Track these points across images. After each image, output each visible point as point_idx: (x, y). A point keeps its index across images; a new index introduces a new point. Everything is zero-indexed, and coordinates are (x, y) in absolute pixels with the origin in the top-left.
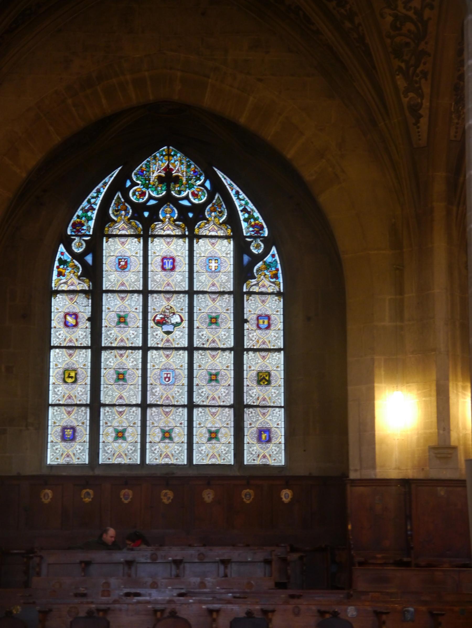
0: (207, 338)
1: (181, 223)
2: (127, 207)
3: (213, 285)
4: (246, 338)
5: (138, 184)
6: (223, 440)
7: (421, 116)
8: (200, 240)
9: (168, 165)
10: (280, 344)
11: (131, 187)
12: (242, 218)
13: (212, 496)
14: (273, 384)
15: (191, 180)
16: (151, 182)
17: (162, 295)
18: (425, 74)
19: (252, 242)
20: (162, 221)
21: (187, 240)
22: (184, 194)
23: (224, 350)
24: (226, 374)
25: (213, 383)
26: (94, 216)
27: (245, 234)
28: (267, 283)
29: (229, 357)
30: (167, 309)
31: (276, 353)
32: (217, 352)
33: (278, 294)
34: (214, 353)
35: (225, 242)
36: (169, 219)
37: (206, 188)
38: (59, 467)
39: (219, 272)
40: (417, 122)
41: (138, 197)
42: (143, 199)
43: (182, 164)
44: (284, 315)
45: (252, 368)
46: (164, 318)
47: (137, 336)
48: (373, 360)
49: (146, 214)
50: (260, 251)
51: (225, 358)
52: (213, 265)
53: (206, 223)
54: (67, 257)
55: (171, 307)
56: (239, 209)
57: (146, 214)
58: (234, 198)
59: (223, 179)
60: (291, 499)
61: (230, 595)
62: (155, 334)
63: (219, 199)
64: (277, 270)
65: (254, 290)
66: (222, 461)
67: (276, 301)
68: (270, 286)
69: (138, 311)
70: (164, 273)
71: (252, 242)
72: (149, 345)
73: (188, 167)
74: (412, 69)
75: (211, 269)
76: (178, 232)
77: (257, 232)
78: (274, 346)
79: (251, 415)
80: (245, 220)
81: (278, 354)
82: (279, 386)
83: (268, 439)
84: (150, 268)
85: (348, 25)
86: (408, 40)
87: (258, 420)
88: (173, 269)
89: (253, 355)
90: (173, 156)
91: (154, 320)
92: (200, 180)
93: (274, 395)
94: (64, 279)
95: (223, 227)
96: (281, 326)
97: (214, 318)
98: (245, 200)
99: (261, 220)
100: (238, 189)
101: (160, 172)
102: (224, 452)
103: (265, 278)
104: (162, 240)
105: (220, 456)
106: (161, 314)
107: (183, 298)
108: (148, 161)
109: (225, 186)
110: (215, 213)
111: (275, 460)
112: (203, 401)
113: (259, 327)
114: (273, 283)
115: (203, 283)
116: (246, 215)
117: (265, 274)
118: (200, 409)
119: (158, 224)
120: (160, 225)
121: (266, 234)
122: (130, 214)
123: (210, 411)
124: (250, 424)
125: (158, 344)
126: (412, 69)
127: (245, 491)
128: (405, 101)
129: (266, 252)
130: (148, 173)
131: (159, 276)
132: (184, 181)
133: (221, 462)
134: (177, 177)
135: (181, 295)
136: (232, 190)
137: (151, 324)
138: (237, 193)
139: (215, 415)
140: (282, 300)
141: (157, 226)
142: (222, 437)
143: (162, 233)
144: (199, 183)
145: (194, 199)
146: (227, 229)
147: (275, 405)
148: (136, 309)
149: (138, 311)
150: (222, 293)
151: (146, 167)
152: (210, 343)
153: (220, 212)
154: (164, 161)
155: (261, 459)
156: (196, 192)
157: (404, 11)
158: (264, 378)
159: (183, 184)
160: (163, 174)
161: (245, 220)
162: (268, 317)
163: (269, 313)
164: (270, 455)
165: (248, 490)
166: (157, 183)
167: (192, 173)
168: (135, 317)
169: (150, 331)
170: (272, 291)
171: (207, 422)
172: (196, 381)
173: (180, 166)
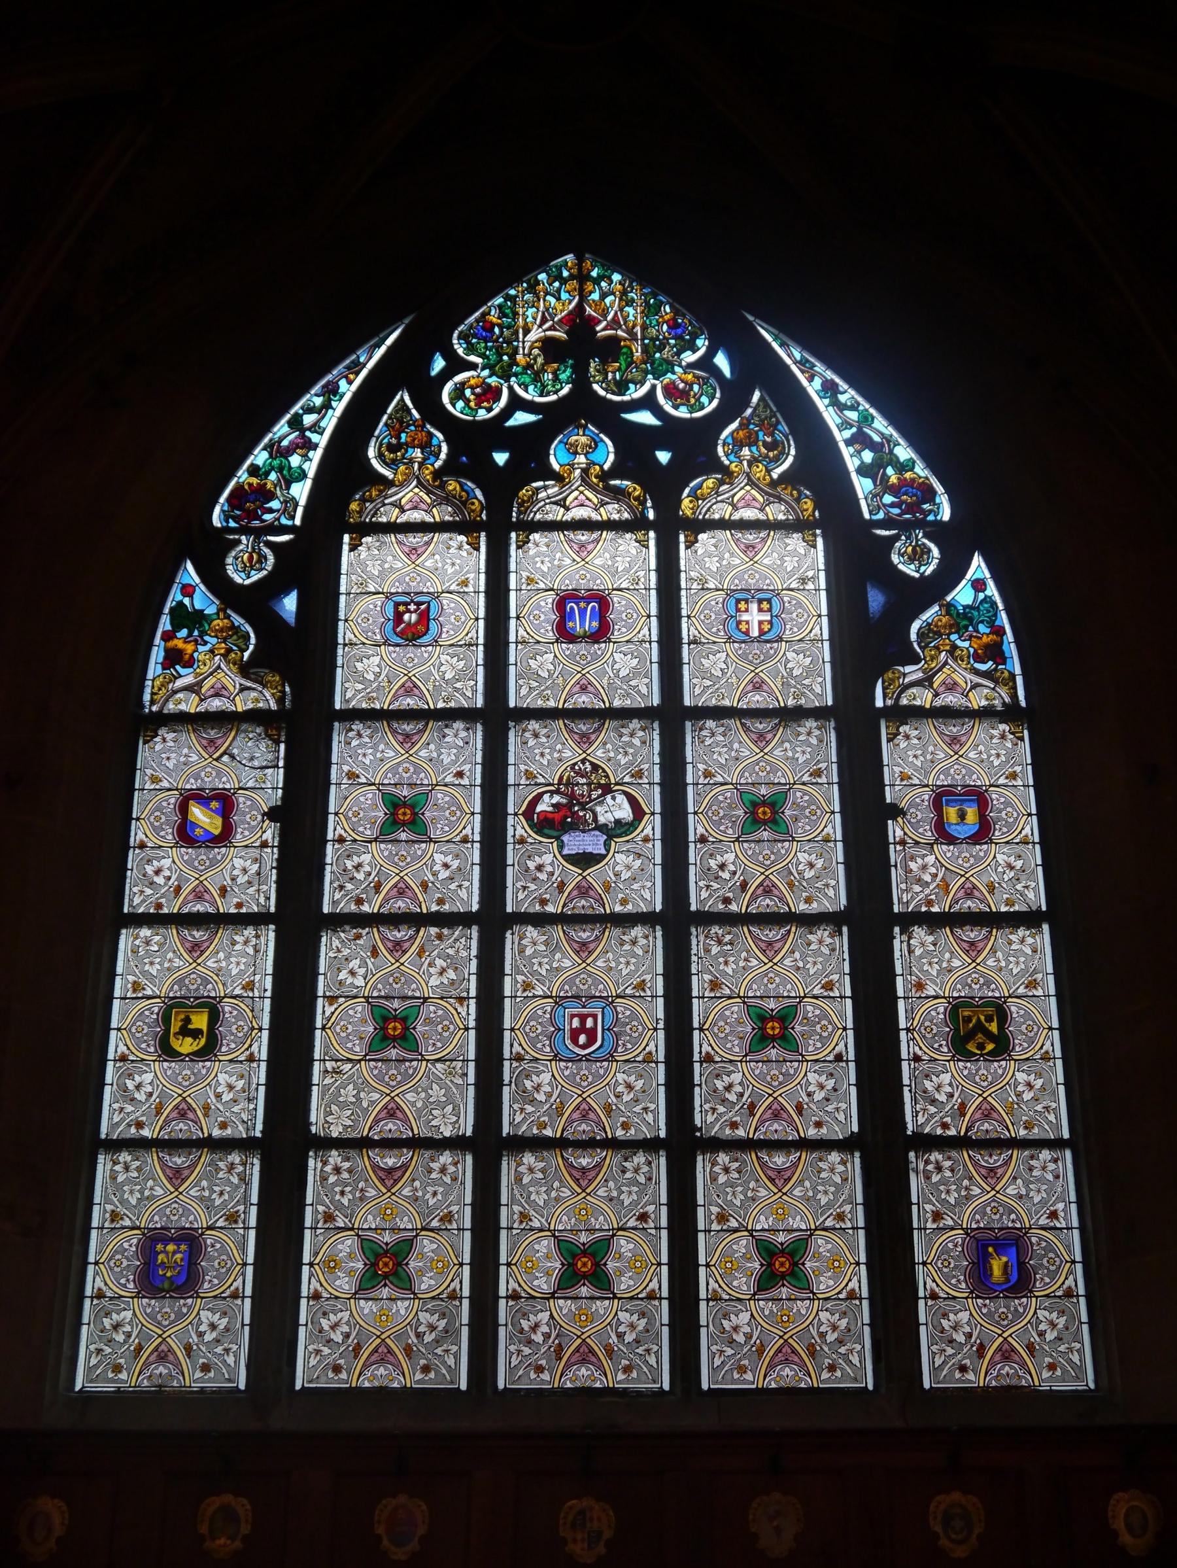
2: (431, 435)
3: (758, 686)
6: (824, 1284)
8: (702, 537)
9: (580, 308)
10: (1035, 895)
11: (446, 375)
12: (852, 464)
16: (519, 357)
19: (896, 538)
20: (559, 478)
22: (636, 393)
23: (810, 921)
24: (824, 1015)
26: (311, 468)
28: (963, 677)
30: (580, 774)
32: (783, 931)
33: (1010, 714)
35: (795, 542)
37: (716, 372)
39: (780, 640)
41: (472, 404)
42: (489, 410)
43: (630, 303)
46: (570, 805)
50: (929, 570)
51: (817, 953)
52: (754, 617)
53: (722, 482)
54: (203, 601)
55: (595, 767)
56: (841, 436)
58: (821, 404)
62: (531, 865)
63: (767, 406)
65: (918, 703)
67: (1003, 737)
68: (975, 686)
69: (465, 781)
73: (650, 310)
75: (747, 633)
76: (613, 511)
77: (912, 508)
78: (1009, 903)
79: (935, 1178)
80: (863, 471)
81: (1028, 933)
82: (1046, 1057)
83: (1014, 1278)
87: (968, 1198)
89: (930, 939)
90: (597, 281)
91: (529, 813)
92: (694, 350)
93: (1027, 1096)
94: (187, 677)
96: (1031, 828)
97: (764, 804)
98: (861, 408)
100: (830, 375)
101: (549, 329)
102: (831, 1337)
103: (955, 659)
105: (812, 1352)
106: (557, 792)
107: (641, 733)
108: (508, 298)
109: (787, 367)
110: (754, 449)
111: (1052, 1367)
112: (734, 1125)
115: (715, 680)
116: (868, 456)
117: (954, 647)
119: (545, 488)
121: (946, 514)
123: (763, 1165)
124: (937, 1216)
129: (951, 573)
132: (638, 355)
133: (824, 1379)
136: (811, 379)
137: (516, 827)
139: (789, 1179)
141: (542, 495)
143: (558, 514)
144: (689, 357)
145: (676, 407)
146: (798, 500)
148: (460, 774)
149: (465, 781)
151: (503, 315)
152: (754, 898)
153: (770, 447)
154: (564, 296)
155: (992, 1364)
158: (980, 1027)
159: (632, 362)
162: (980, 797)
163: (980, 779)
164: (1030, 1348)
166: (540, 360)
168: (454, 801)
170: (984, 703)
173: (621, 310)
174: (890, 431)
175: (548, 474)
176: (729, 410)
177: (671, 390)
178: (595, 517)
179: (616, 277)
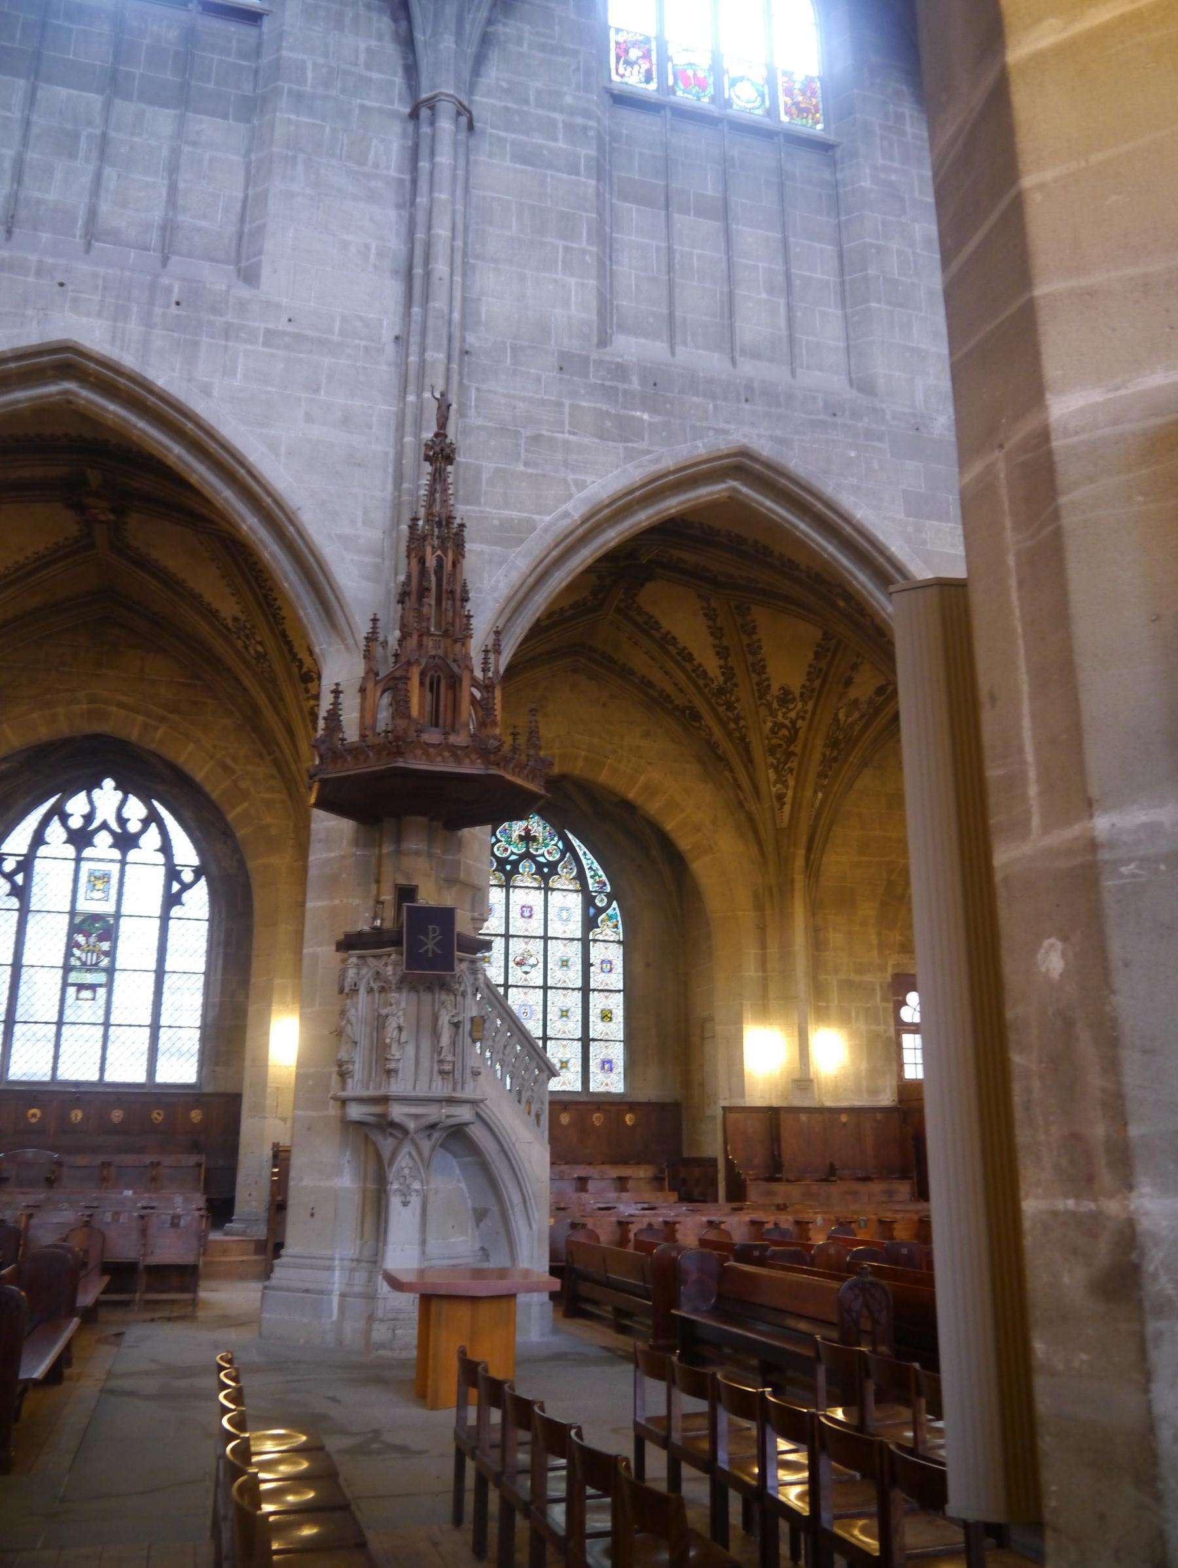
3: (565, 932)
4: (591, 980)
7: (785, 804)
14: (614, 1020)
17: (521, 939)
18: (791, 770)
21: (543, 892)
22: (540, 852)
23: (573, 989)
25: (564, 1019)
28: (610, 933)
33: (619, 942)
34: (565, 992)
35: (575, 894)
40: (781, 808)
44: (624, 960)
47: (618, 981)
48: (741, 1005)
52: (564, 915)
56: (586, 867)
57: (508, 867)
58: (582, 858)
73: (545, 828)
74: (781, 766)
76: (535, 884)
77: (601, 888)
80: (592, 877)
85: (732, 725)
86: (781, 742)
88: (530, 917)
96: (621, 970)
99: (604, 878)
104: (522, 891)
113: (602, 971)
116: (592, 873)
118: (553, 1041)
120: (519, 877)
126: (781, 766)
127: (596, 1115)
128: (774, 790)
129: (609, 905)
132: (541, 841)
134: (535, 836)
137: (511, 964)
144: (553, 842)
150: (573, 939)
160: (523, 834)
161: (592, 877)
162: (610, 962)
169: (510, 970)
174: (599, 867)
175: (519, 873)
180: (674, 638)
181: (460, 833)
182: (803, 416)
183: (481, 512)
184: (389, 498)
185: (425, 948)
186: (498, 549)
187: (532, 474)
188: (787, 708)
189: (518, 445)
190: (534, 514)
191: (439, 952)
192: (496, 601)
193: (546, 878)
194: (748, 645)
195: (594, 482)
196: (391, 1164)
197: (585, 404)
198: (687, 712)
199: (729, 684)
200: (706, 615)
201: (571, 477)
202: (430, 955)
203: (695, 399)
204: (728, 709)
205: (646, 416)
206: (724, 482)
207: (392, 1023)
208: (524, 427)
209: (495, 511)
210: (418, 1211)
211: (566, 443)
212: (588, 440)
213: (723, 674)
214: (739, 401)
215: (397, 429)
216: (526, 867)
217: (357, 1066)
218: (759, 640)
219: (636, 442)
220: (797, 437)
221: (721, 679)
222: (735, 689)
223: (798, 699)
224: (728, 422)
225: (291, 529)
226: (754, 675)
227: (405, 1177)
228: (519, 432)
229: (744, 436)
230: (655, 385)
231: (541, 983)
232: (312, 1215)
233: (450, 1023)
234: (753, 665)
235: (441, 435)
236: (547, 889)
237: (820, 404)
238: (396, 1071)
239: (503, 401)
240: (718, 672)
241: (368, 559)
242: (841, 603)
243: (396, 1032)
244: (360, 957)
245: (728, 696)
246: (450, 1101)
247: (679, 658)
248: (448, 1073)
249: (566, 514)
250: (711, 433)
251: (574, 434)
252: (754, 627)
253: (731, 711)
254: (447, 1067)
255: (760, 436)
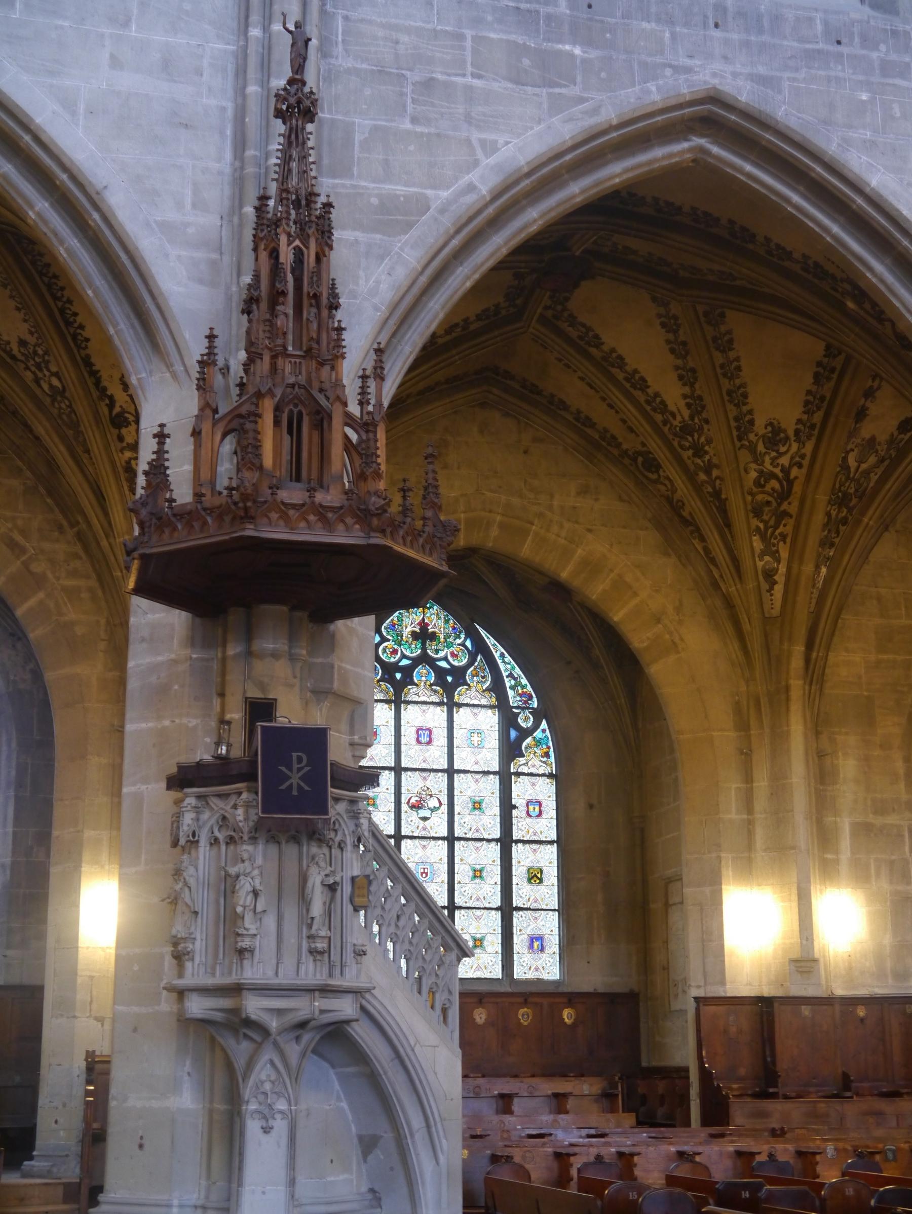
0: (469, 826)
1: (438, 688)
3: (476, 763)
4: (514, 827)
5: (389, 640)
7: (775, 583)
9: (423, 619)
12: (508, 685)
13: (484, 1017)
14: (546, 882)
15: (449, 637)
17: (417, 773)
19: (520, 713)
20: (417, 685)
22: (441, 654)
23: (489, 841)
24: (492, 870)
25: (477, 881)
27: (511, 705)
28: (538, 763)
29: (495, 850)
31: (549, 846)
33: (550, 776)
34: (478, 844)
36: (425, 683)
38: (527, 982)
39: (483, 747)
40: (772, 588)
43: (440, 618)
44: (557, 801)
45: (522, 864)
48: (719, 858)
49: (398, 676)
50: (529, 725)
51: (491, 851)
52: (476, 739)
53: (467, 690)
55: (428, 788)
56: (505, 674)
58: (499, 661)
59: (485, 638)
60: (575, 1019)
61: (645, 1135)
62: (409, 820)
64: (549, 748)
66: (489, 974)
68: (541, 766)
69: (389, 791)
70: (420, 747)
71: (520, 713)
72: (403, 834)
73: (447, 622)
74: (770, 531)
76: (435, 699)
77: (526, 702)
78: (546, 837)
79: (521, 919)
80: (512, 688)
83: (540, 948)
84: (403, 740)
85: (702, 477)
86: (770, 499)
88: (430, 742)
90: (429, 609)
91: (408, 803)
92: (460, 638)
95: (487, 694)
96: (553, 814)
100: (503, 650)
101: (414, 627)
108: (400, 613)
112: (466, 902)
114: (544, 762)
118: (463, 911)
120: (414, 689)
121: (535, 705)
122: (380, 675)
125: (413, 832)
126: (770, 531)
127: (522, 1011)
128: (760, 564)
130: (400, 628)
131: (414, 750)
132: (442, 640)
133: (488, 976)
134: (434, 633)
135: (440, 774)
136: (496, 652)
137: (404, 807)
138: (502, 655)
140: (554, 783)
141: (411, 691)
142: (488, 946)
143: (416, 699)
144: (458, 641)
147: (549, 907)
148: (387, 789)
149: (389, 791)
150: (487, 773)
151: (399, 620)
152: (473, 833)
153: (483, 677)
154: (418, 614)
156: (456, 653)
157: (771, 468)
158: (535, 875)
161: (512, 688)
163: (540, 798)
164: (543, 968)
165: (525, 1009)
166: (411, 639)
167: (451, 629)
168: (386, 798)
169: (403, 816)
170: (543, 772)
171: (471, 927)
172: (457, 878)
174: (521, 673)
176: (471, 663)
177: (453, 654)
178: (428, 700)
179: (435, 607)
180: (620, 357)
181: (332, 627)
182: (796, 44)
183: (354, 187)
184: (228, 170)
185: (287, 784)
186: (378, 236)
187: (422, 133)
188: (777, 451)
189: (402, 94)
190: (425, 188)
191: (307, 788)
192: (376, 309)
193: (449, 690)
194: (722, 366)
195: (507, 143)
196: (246, 1077)
197: (493, 35)
198: (640, 459)
199: (696, 420)
200: (663, 325)
201: (476, 136)
202: (295, 793)
203: (645, 25)
204: (695, 455)
205: (577, 51)
206: (687, 140)
207: (245, 886)
208: (410, 70)
209: (372, 185)
210: (284, 1141)
211: (469, 88)
212: (499, 86)
213: (688, 406)
214: (705, 25)
215: (237, 75)
216: (423, 674)
217: (198, 943)
218: (737, 359)
219: (565, 86)
220: (787, 75)
221: (686, 413)
222: (706, 427)
223: (793, 438)
224: (691, 57)
225: (96, 216)
226: (730, 407)
227: (265, 1094)
228: (403, 75)
229: (714, 75)
230: (590, 6)
231: (444, 833)
232: (141, 1146)
233: (323, 884)
234: (729, 393)
235: (297, 81)
236: (451, 706)
237: (820, 28)
238: (251, 951)
239: (381, 33)
240: (682, 403)
241: (199, 255)
242: (850, 305)
243: (250, 897)
244: (199, 797)
245: (696, 436)
246: (325, 990)
247: (628, 385)
248: (321, 953)
249: (471, 188)
250: (668, 72)
251: (479, 77)
252: (731, 341)
253: (700, 457)
254: (320, 945)
255: (735, 75)
